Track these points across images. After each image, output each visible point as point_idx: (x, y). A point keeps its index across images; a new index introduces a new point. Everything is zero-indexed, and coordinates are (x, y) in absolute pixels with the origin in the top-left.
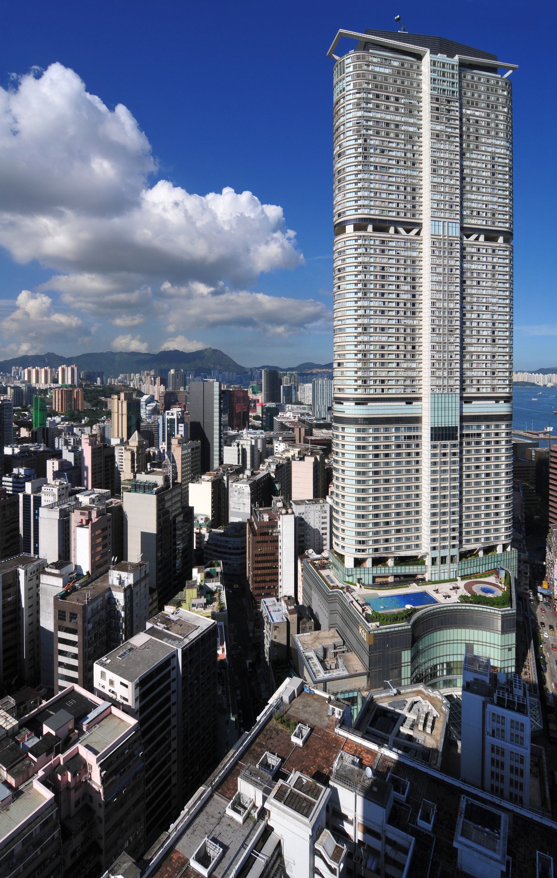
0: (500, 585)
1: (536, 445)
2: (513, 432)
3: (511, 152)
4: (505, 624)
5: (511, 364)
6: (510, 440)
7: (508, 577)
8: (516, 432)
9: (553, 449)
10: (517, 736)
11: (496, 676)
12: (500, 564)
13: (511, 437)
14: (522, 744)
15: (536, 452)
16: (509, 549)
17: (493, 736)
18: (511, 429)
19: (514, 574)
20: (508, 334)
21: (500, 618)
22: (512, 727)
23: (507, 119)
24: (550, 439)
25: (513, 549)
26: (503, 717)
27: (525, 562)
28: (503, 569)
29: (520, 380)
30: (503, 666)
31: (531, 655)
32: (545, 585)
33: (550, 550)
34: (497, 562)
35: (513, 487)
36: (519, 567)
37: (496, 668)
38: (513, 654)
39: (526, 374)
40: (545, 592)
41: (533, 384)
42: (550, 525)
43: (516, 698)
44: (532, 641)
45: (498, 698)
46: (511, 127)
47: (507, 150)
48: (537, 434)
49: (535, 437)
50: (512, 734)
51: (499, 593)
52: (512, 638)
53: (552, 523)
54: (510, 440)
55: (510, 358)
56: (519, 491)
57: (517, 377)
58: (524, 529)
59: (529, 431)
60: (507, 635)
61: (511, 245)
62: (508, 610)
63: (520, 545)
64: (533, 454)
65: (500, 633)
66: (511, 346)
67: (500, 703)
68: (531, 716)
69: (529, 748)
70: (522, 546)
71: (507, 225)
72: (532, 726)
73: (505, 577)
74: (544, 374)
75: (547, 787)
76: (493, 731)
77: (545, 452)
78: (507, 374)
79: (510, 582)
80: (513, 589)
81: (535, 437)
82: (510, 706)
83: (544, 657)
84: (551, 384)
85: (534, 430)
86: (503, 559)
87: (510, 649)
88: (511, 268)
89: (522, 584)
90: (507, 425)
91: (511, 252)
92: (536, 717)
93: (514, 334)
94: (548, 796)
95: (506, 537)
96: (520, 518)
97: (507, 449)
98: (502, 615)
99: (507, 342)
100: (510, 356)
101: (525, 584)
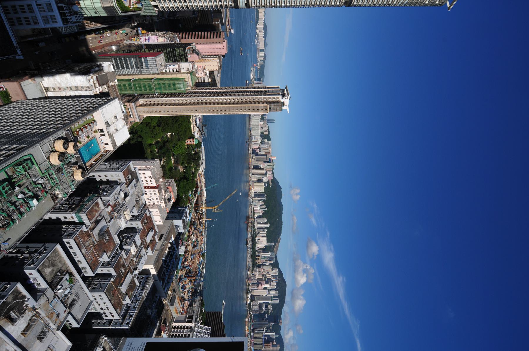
0: (132, 5)
1: (222, 24)
2: (228, 9)
3: (400, 6)
4: (109, 9)
5: (269, 7)
6: (222, 8)
7: (139, 10)
8: (228, 12)
9: (221, 33)
10: (48, 20)
11: (75, 4)
12: (144, 4)
13: (225, 8)
14: (45, 23)
15: (218, 24)
16: (156, 9)
17: (37, 5)
18: (229, 8)
19: (142, 13)
20: (288, 4)
21: (111, 6)
22: (51, 16)
23: (421, 3)
24: (227, 31)
25: (157, 12)
26: (52, 11)
27: (152, 20)
28: (142, 6)
29: (260, 14)
30: (83, 9)
31: (99, 26)
32: (144, 32)
33: (164, 34)
34: (145, 2)
35: (194, 11)
36: (148, 16)
37: (80, 5)
38: (94, 15)
39: (263, 17)
40: (139, 32)
41: (257, 22)
42: (178, 33)
43: (69, 18)
44: (108, 26)
45: (62, 6)
46: (415, 6)
47: (402, 3)
48: (228, 25)
49: (227, 24)
50: (46, 16)
51: (127, 4)
52: (103, 14)
53: (180, 34)
54: (222, 8)
55: (273, 6)
56: (193, 15)
57: (261, 10)
58: (171, 18)
59: (230, 20)
60: (103, 10)
61: (342, 6)
62: (119, 11)
63: (161, 16)
64: (217, 23)
65: (102, 6)
66: (280, 6)
67: (60, 9)
68: (65, 27)
69: (45, 27)
70: (161, 18)
71: (355, 3)
72: (60, 28)
73: (138, 8)
74: (264, 28)
75: (32, 39)
76: (40, 5)
77: (219, 29)
78: (263, 5)
79: (136, 11)
80: (133, 13)
81: (227, 24)
82: (62, 15)
83: (103, 33)
84: (258, 32)
85: (231, 23)
86: (148, 6)
87: (96, 13)
88: (329, 6)
89: (139, 19)
90: (232, 6)
91: (338, 6)
92: (66, 30)
93: (288, 9)
94: (28, 39)
95: (163, 7)
96: (177, 16)
97: (217, 6)
98: (114, 6)
99: (283, 4)
100: (274, 6)
101: (139, 20)
